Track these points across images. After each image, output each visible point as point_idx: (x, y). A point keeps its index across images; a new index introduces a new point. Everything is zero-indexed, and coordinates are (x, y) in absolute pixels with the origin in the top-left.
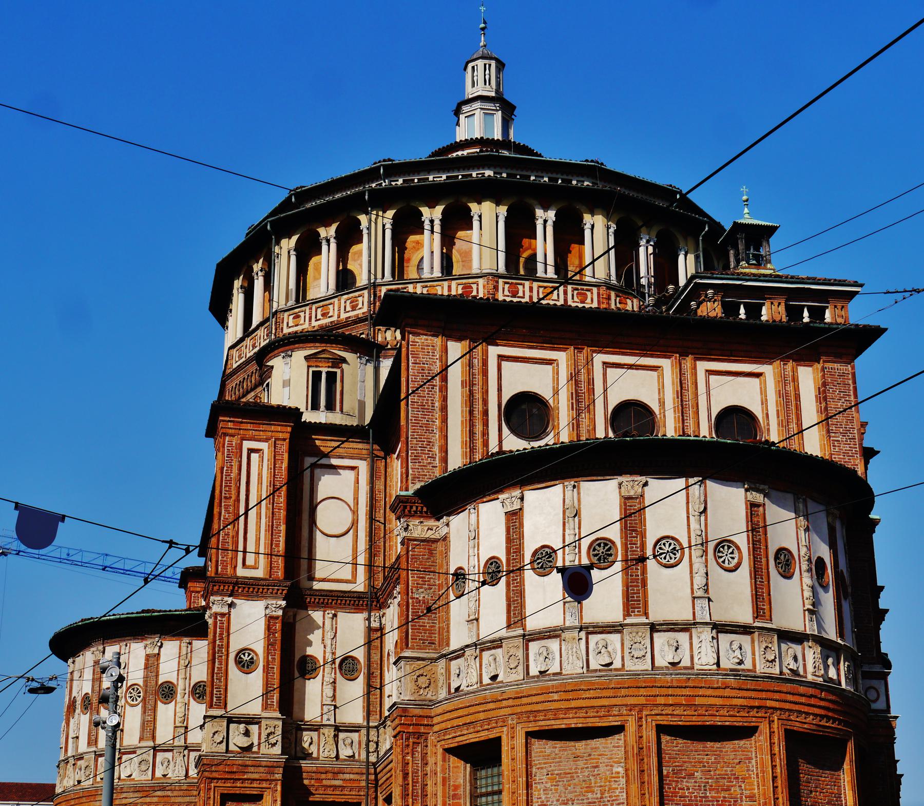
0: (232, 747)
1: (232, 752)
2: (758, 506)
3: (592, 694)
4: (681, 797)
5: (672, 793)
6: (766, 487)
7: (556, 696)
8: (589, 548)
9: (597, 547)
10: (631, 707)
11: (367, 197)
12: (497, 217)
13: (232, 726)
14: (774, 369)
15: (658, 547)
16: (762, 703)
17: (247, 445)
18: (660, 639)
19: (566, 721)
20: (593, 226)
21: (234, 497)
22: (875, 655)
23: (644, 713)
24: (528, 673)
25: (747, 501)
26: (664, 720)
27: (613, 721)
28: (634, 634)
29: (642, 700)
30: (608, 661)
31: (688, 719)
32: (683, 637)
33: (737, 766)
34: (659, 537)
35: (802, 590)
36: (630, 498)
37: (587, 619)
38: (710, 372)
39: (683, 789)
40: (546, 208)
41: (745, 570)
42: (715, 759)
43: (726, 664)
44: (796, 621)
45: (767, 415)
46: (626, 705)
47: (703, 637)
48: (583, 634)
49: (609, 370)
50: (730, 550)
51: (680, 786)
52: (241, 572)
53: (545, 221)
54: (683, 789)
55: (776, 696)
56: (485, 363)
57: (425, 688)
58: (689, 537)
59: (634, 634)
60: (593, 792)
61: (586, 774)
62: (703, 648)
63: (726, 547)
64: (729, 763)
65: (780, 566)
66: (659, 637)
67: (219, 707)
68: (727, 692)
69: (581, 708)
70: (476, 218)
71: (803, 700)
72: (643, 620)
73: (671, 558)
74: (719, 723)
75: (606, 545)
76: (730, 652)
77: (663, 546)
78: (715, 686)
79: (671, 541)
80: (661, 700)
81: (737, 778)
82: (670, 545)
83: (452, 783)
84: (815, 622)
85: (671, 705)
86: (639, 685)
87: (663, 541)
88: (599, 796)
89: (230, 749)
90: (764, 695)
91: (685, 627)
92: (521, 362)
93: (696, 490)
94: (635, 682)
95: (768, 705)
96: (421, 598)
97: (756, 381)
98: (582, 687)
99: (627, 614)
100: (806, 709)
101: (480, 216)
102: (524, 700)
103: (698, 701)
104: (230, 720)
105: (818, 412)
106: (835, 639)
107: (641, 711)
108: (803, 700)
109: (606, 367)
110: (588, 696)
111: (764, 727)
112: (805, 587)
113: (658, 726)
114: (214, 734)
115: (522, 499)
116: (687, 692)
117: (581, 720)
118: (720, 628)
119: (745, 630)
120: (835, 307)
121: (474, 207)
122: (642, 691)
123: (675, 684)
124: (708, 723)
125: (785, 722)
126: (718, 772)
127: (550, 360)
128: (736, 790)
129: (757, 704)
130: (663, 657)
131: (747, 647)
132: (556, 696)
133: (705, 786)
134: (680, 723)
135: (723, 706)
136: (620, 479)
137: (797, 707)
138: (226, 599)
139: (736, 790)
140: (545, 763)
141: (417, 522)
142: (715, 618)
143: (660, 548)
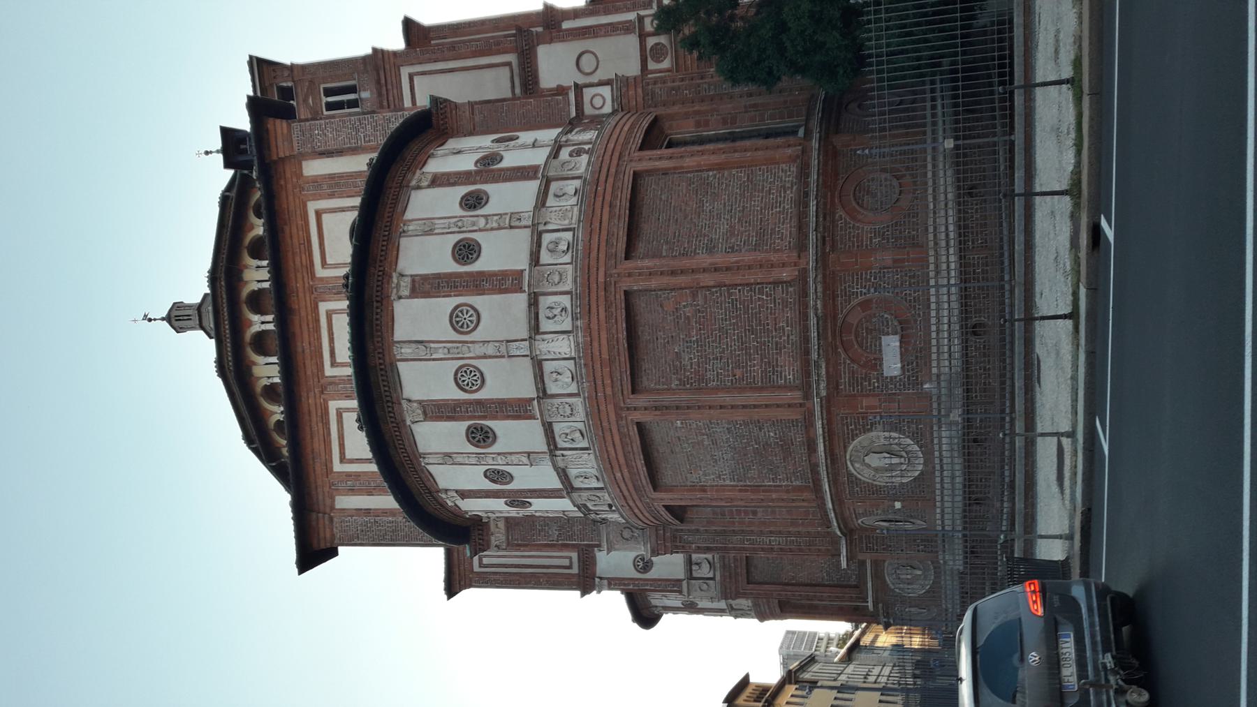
0: (711, 575)
1: (715, 575)
2: (413, 281)
3: (611, 449)
4: (699, 367)
5: (695, 375)
6: (394, 275)
7: (618, 475)
8: (477, 447)
9: (477, 439)
10: (619, 417)
11: (274, 464)
12: (267, 364)
13: (695, 574)
14: (310, 200)
15: (467, 388)
16: (602, 286)
17: (476, 568)
18: (552, 389)
19: (640, 467)
20: (259, 281)
21: (518, 578)
22: (561, 98)
23: (622, 405)
24: (601, 489)
25: (410, 297)
26: (628, 386)
27: (634, 431)
28: (550, 413)
29: (611, 408)
30: (578, 435)
31: (623, 365)
32: (548, 367)
33: (666, 309)
34: (456, 388)
35: (492, 229)
36: (425, 413)
37: (545, 448)
38: (324, 264)
39: (691, 364)
40: (250, 324)
41: (478, 301)
42: (660, 331)
43: (567, 325)
44: (522, 238)
45: (352, 207)
46: (617, 421)
47: (544, 350)
48: (558, 453)
49: (338, 360)
50: (460, 314)
51: (689, 367)
52: (575, 570)
53: (263, 323)
54: (691, 364)
55: (594, 270)
56: (349, 475)
57: (632, 532)
58: (452, 359)
59: (550, 413)
60: (703, 441)
61: (686, 445)
62: (557, 350)
63: (458, 319)
64: (663, 318)
65: (470, 256)
66: (551, 390)
67: (681, 586)
68: (594, 326)
69: (625, 456)
70: (271, 381)
71: (596, 238)
72: (535, 402)
73: (475, 375)
74: (625, 333)
75: (473, 432)
76: (556, 319)
77: (466, 383)
78: (589, 339)
79: (459, 375)
80: (609, 391)
81: (676, 309)
82: (462, 376)
83: (711, 516)
84: (522, 214)
85: (612, 381)
86: (596, 411)
87: (460, 382)
88: (705, 437)
89: (712, 576)
90: (594, 286)
91: (538, 365)
92: (343, 441)
93: (407, 351)
94: (595, 413)
95: (603, 280)
96: (557, 533)
97: (325, 217)
98: (606, 456)
99: (533, 417)
100: (604, 233)
101: (269, 377)
102: (626, 493)
103: (605, 356)
104: (690, 577)
105: (341, 156)
106: (539, 182)
107: (621, 409)
108: (596, 238)
109: (335, 363)
110: (613, 451)
111: (625, 284)
112: (488, 226)
113: (633, 392)
114: (701, 590)
115: (446, 491)
116: (598, 366)
117: (637, 457)
118: (535, 328)
119: (533, 303)
120: (274, 78)
121: (265, 382)
122: (603, 408)
123: (592, 378)
124: (626, 345)
125: (619, 259)
126: (673, 327)
127: (337, 415)
128: (689, 311)
129: (603, 293)
130: (569, 386)
131: (551, 299)
132: (618, 475)
133: (687, 342)
134: (628, 373)
135: (608, 330)
136: (408, 423)
137: (603, 244)
138: (597, 583)
139: (689, 311)
140: (681, 474)
141: (493, 538)
142: (525, 335)
143: (468, 385)
